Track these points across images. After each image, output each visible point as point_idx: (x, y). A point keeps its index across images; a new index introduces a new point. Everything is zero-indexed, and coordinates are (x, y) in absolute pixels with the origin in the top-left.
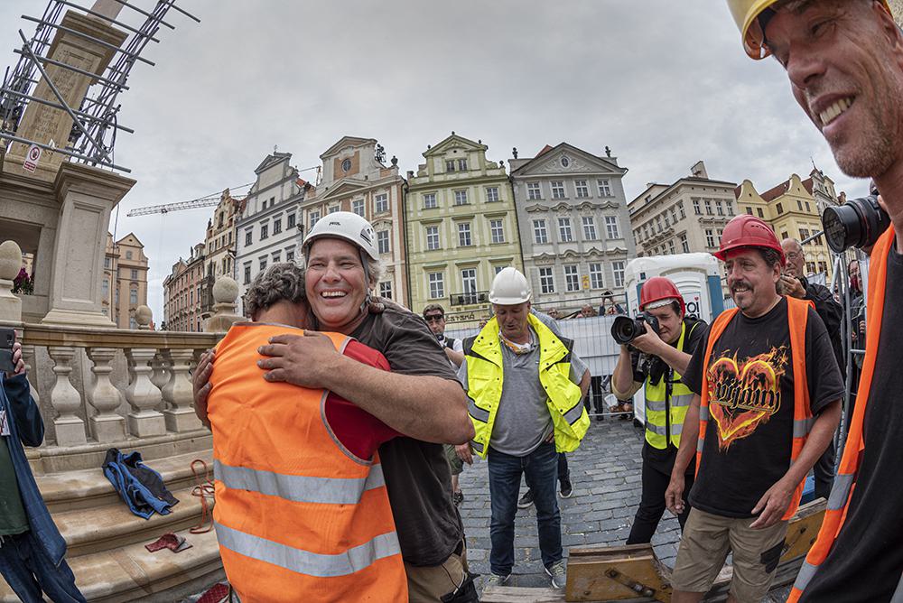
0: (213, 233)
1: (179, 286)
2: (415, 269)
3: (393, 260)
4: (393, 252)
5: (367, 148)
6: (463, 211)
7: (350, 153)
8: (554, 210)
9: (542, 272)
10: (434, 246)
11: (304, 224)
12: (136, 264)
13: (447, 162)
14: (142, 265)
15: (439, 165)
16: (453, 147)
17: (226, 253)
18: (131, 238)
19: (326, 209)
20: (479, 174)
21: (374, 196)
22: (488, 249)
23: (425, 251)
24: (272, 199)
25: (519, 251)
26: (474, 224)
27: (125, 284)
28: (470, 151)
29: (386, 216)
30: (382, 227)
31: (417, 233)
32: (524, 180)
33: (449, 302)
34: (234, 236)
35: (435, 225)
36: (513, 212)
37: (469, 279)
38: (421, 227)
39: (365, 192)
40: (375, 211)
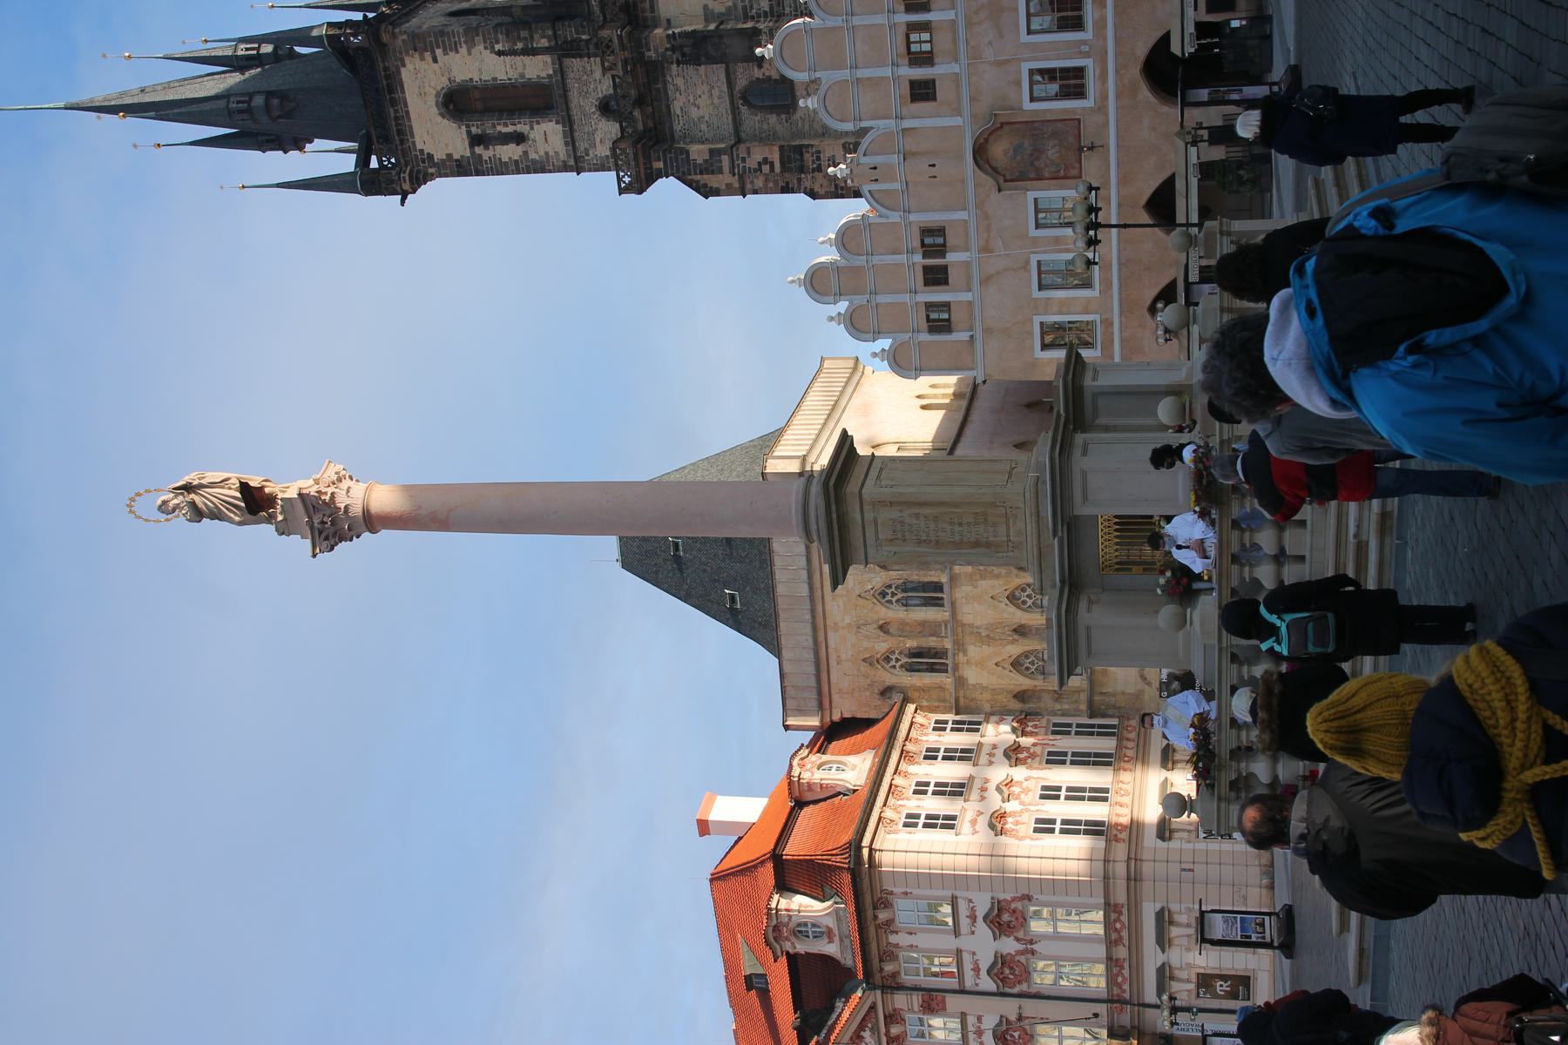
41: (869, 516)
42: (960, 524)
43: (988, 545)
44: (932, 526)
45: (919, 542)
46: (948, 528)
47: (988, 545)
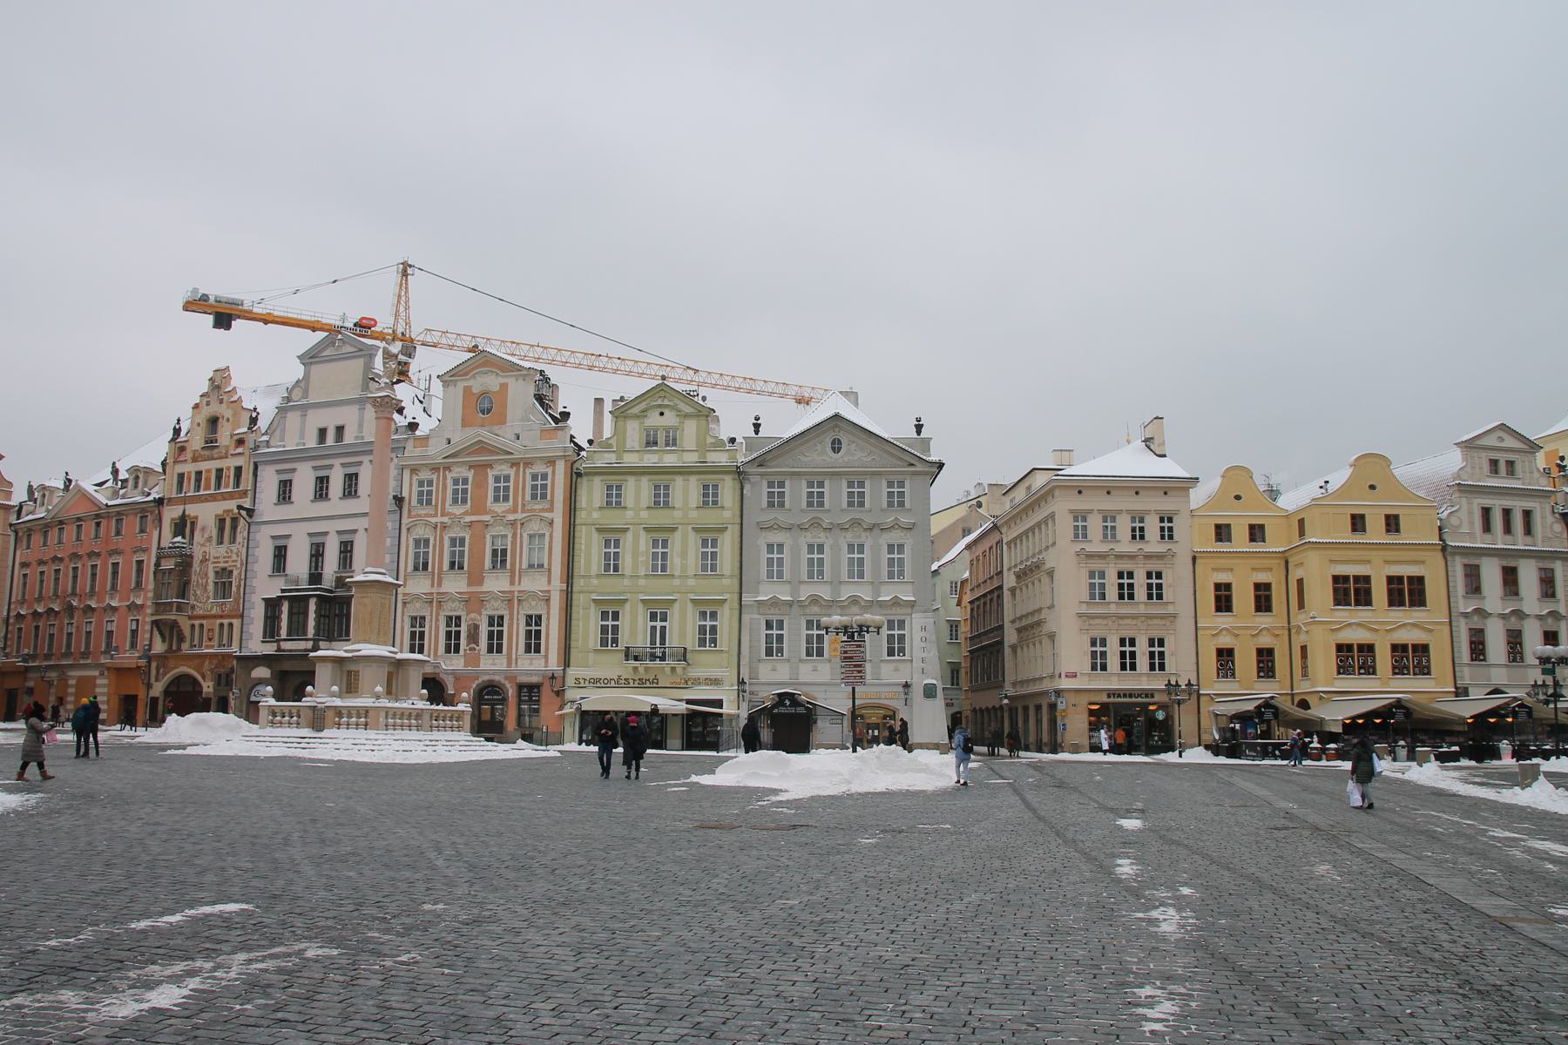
0: (188, 455)
2: (579, 600)
3: (549, 582)
4: (549, 570)
5: (521, 381)
6: (662, 518)
7: (491, 382)
8: (801, 528)
9: (769, 625)
10: (612, 565)
11: (405, 494)
13: (647, 431)
15: (634, 433)
16: (660, 406)
17: (232, 505)
19: (445, 478)
20: (691, 459)
21: (528, 471)
22: (692, 582)
23: (598, 576)
24: (340, 430)
25: (737, 588)
26: (676, 540)
28: (687, 416)
29: (542, 510)
30: (535, 527)
31: (589, 546)
32: (762, 475)
33: (622, 655)
34: (247, 476)
35: (616, 536)
36: (737, 527)
37: (659, 624)
38: (595, 535)
39: (515, 464)
40: (528, 497)
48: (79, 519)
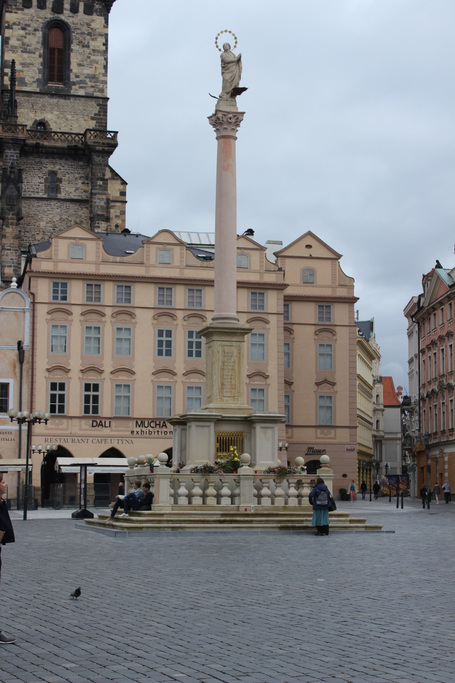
1: (440, 322)
12: (327, 293)
14: (342, 292)
18: (309, 241)
27: (305, 337)
41: (234, 344)
42: (231, 379)
43: (222, 389)
44: (230, 368)
45: (223, 362)
46: (230, 374)
47: (222, 389)
48: (441, 303)
